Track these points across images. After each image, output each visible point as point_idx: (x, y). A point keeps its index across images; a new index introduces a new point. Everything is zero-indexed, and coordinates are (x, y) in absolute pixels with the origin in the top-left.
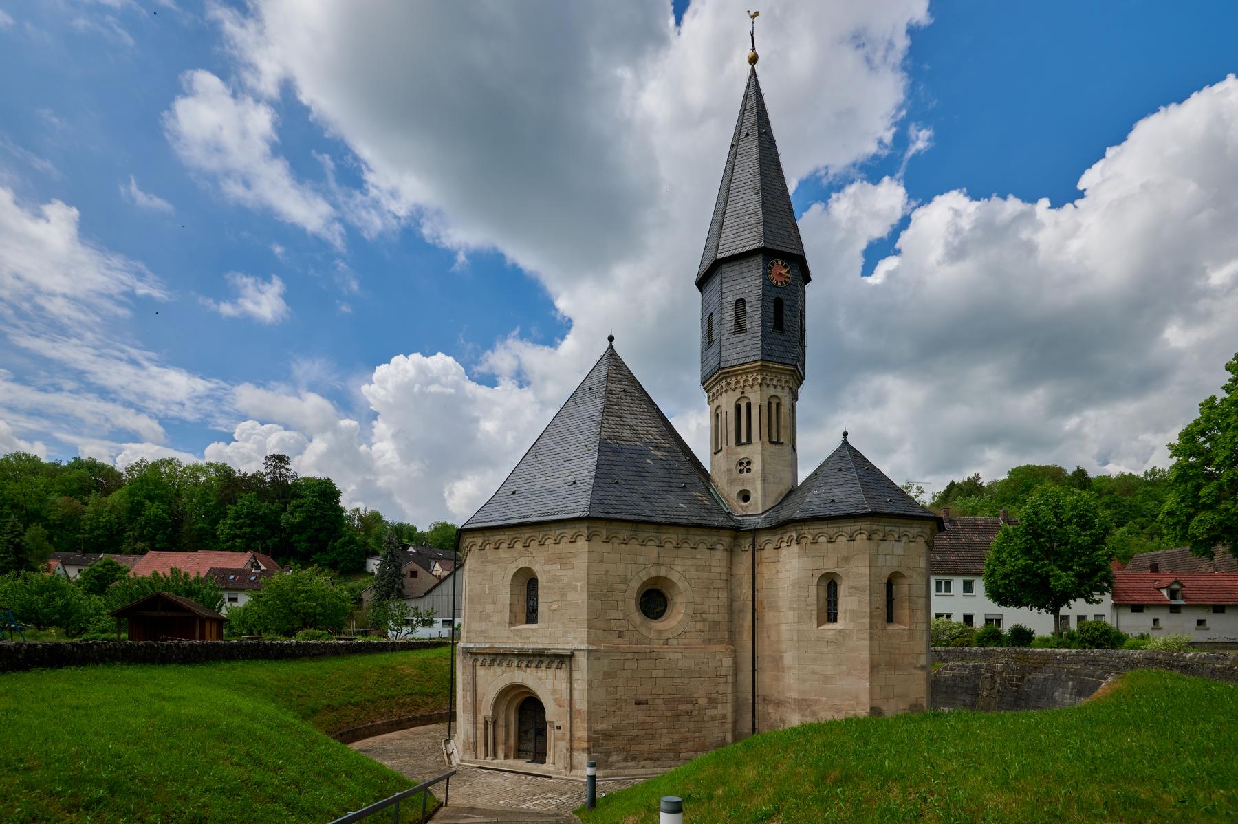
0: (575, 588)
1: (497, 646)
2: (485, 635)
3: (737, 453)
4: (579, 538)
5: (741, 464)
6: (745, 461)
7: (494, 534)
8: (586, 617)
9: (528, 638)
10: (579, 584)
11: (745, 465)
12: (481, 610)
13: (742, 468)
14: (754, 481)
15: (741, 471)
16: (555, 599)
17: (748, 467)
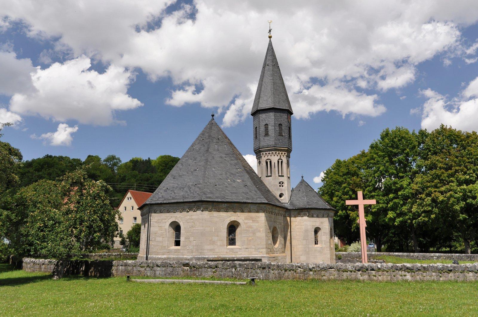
0: (260, 231)
1: (222, 256)
2: (214, 251)
3: (279, 179)
4: (261, 210)
5: (280, 183)
6: (281, 183)
7: (218, 204)
8: (265, 243)
9: (237, 252)
10: (261, 230)
11: (281, 183)
12: (210, 239)
13: (280, 185)
14: (285, 190)
15: (280, 186)
16: (250, 235)
17: (282, 185)
